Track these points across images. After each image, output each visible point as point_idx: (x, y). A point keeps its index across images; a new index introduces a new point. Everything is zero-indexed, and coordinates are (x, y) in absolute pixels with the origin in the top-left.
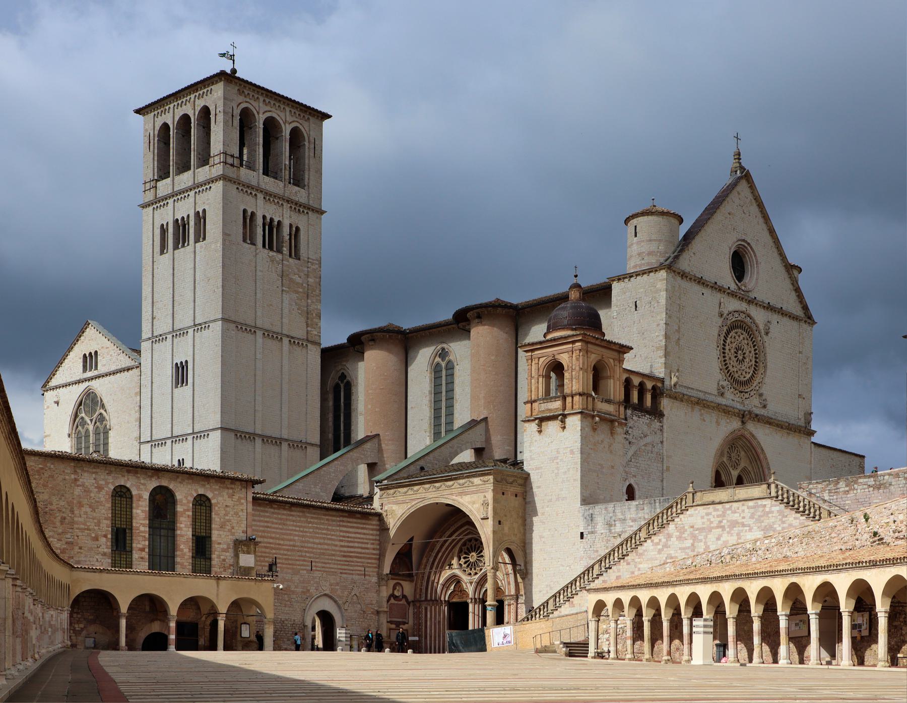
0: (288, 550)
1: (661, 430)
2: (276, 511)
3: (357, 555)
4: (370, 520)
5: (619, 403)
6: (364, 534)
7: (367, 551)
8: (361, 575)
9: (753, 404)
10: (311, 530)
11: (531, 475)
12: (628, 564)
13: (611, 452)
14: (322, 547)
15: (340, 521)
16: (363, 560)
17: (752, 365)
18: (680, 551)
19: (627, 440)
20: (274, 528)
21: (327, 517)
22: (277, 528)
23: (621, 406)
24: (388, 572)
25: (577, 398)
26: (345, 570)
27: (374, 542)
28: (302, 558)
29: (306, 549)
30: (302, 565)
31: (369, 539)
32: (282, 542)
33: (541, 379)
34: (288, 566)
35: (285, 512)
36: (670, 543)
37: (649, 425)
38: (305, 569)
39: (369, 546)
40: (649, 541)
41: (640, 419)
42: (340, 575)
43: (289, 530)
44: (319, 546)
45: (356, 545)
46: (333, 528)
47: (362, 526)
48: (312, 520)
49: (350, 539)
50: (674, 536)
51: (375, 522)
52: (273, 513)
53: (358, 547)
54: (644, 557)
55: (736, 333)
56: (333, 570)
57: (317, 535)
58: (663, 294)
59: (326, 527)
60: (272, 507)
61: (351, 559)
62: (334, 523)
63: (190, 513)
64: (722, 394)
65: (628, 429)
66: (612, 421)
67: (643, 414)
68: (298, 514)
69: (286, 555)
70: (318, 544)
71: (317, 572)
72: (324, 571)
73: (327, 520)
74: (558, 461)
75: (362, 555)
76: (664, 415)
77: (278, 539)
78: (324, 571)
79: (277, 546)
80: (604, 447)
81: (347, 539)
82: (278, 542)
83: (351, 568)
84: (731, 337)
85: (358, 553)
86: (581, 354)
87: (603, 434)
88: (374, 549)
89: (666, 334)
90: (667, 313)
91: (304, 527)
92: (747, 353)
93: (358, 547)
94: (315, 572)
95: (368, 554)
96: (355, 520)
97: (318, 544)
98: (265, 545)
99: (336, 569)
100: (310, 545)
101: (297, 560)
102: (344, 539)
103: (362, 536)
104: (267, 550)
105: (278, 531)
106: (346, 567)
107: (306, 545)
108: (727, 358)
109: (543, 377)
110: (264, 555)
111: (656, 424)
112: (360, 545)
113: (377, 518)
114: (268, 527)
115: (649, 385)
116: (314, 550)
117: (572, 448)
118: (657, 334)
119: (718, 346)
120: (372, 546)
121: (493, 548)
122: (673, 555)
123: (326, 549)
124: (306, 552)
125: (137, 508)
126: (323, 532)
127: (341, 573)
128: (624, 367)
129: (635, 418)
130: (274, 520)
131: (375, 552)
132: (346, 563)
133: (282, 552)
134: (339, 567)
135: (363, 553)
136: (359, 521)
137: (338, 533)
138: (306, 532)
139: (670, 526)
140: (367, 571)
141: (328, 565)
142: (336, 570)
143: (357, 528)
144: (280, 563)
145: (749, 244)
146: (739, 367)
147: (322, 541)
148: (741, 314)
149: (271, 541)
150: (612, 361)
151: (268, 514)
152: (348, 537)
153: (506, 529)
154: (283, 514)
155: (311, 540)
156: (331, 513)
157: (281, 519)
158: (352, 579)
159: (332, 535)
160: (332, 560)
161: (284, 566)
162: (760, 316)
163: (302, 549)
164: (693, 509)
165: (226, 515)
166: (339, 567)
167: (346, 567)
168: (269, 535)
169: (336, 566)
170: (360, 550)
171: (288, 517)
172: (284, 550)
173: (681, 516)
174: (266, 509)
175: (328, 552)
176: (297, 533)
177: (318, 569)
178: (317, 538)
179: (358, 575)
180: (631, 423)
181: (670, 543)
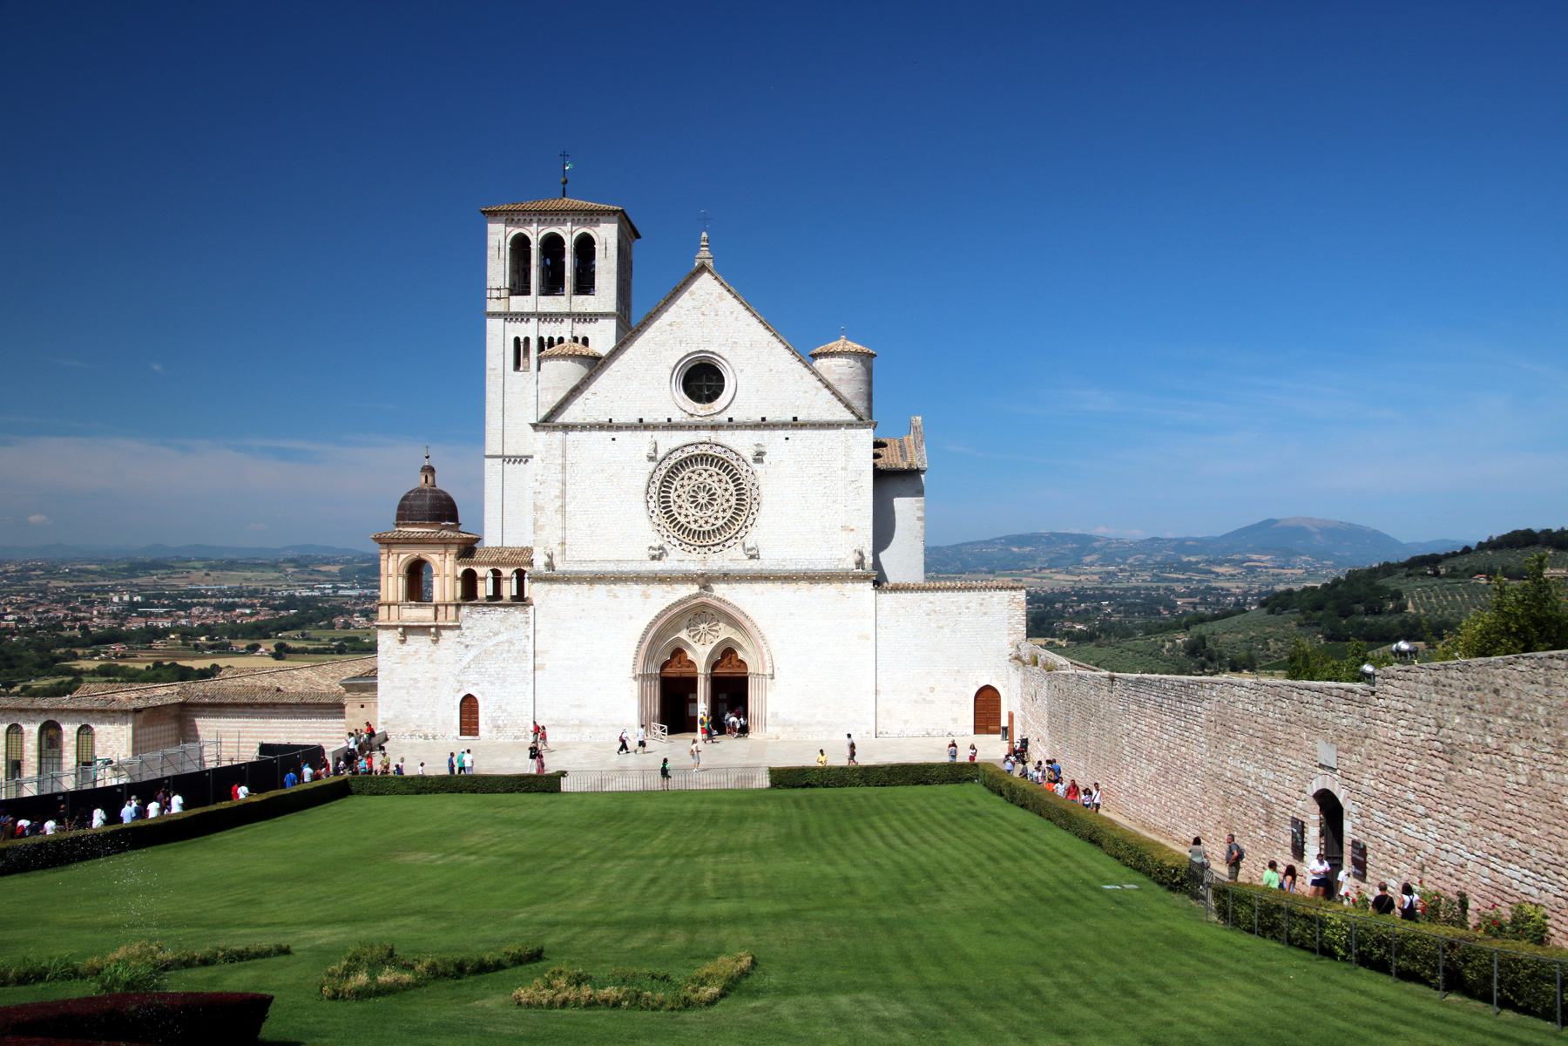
1: (527, 623)
9: (729, 558)
13: (432, 662)
17: (730, 507)
19: (462, 643)
33: (400, 579)
37: (502, 621)
41: (487, 616)
55: (693, 472)
63: (75, 743)
64: (653, 558)
84: (683, 479)
87: (418, 643)
92: (719, 492)
108: (674, 508)
111: (516, 615)
119: (651, 497)
125: (28, 742)
129: (476, 616)
145: (713, 353)
146: (701, 514)
147: (314, 735)
148: (700, 447)
149: (251, 740)
162: (742, 443)
165: (107, 741)
178: (308, 732)
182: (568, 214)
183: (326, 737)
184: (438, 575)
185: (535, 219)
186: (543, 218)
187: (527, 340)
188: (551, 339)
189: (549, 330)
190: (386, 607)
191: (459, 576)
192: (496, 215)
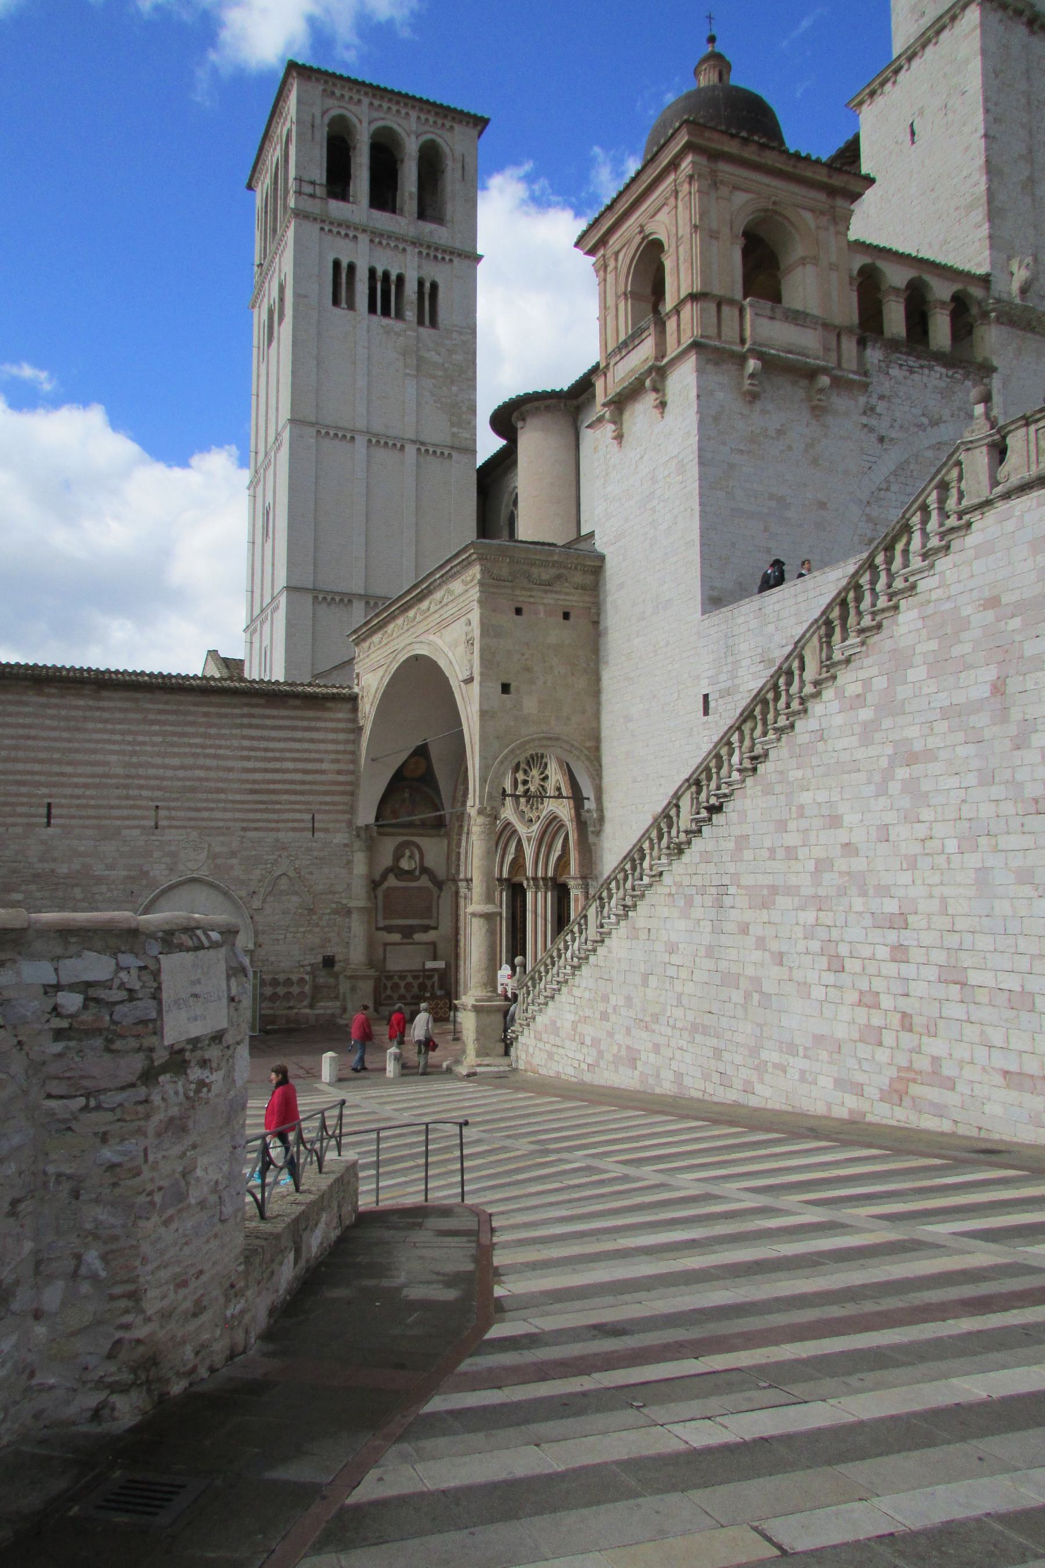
0: (86, 786)
2: (53, 701)
3: (294, 787)
4: (330, 709)
5: (839, 332)
6: (312, 741)
7: (318, 777)
8: (303, 830)
10: (160, 739)
11: (607, 559)
12: (768, 791)
13: (815, 462)
14: (189, 773)
15: (243, 716)
16: (310, 798)
18: (942, 726)
19: (872, 430)
20: (44, 739)
21: (205, 709)
22: (56, 740)
23: (844, 339)
24: (371, 819)
25: (687, 311)
26: (258, 821)
27: (339, 757)
28: (131, 802)
29: (142, 782)
30: (128, 818)
31: (327, 752)
32: (69, 769)
34: (87, 822)
35: (81, 703)
36: (902, 692)
38: (138, 827)
39: (325, 766)
40: (828, 694)
42: (242, 833)
43: (89, 741)
44: (181, 773)
45: (289, 765)
46: (223, 731)
47: (305, 724)
48: (159, 717)
49: (270, 755)
50: (918, 659)
51: (342, 713)
52: (46, 706)
53: (296, 771)
54: (815, 760)
56: (221, 824)
57: (176, 750)
58: (976, 65)
59: (202, 730)
60: (40, 694)
61: (274, 797)
62: (224, 721)
65: (874, 401)
66: (811, 374)
67: (924, 363)
68: (119, 704)
69: (78, 797)
70: (175, 768)
71: (173, 831)
72: (192, 827)
73: (206, 715)
74: (656, 501)
75: (307, 787)
76: (994, 370)
77: (52, 761)
78: (192, 827)
79: (56, 779)
80: (790, 448)
81: (263, 754)
82: (56, 769)
83: (275, 816)
85: (292, 782)
86: (695, 186)
88: (339, 772)
89: (987, 161)
90: (987, 111)
91: (136, 733)
93: (296, 771)
94: (167, 831)
95: (322, 783)
96: (286, 713)
97: (175, 768)
98: (19, 777)
99: (229, 820)
100: (152, 772)
101: (112, 807)
102: (252, 754)
103: (305, 746)
104: (24, 790)
105: (58, 744)
106: (258, 816)
107: (141, 771)
109: (626, 299)
110: (14, 800)
112: (300, 765)
113: (349, 706)
114: (29, 738)
115: (942, 291)
116: (165, 783)
117: (680, 457)
118: (965, 173)
120: (335, 767)
121: (482, 758)
122: (918, 746)
123: (200, 779)
124: (141, 787)
126: (192, 741)
127: (244, 829)
128: (853, 235)
129: (895, 371)
130: (48, 722)
131: (341, 778)
132: (262, 806)
133: (68, 791)
134: (238, 815)
135: (310, 783)
136: (298, 713)
137: (235, 743)
138: (144, 743)
139: (901, 618)
140: (320, 821)
141: (206, 814)
142: (230, 824)
143: (294, 728)
144: (61, 816)
147: (190, 761)
149: (37, 767)
150: (808, 216)
151: (30, 709)
152: (266, 750)
153: (530, 705)
154: (77, 708)
155: (159, 761)
156: (216, 699)
157: (67, 719)
158: (277, 840)
159: (220, 747)
160: (219, 801)
161: (73, 822)
163: (129, 781)
164: (991, 515)
166: (238, 815)
167: (258, 816)
168: (32, 755)
169: (229, 815)
170: (298, 777)
171: (88, 714)
172: (76, 785)
173: (943, 563)
174: (25, 698)
175: (205, 784)
176: (116, 747)
177: (175, 823)
178: (175, 755)
179: (294, 830)
180: (881, 384)
181: (902, 692)
182: (413, 107)
183: (218, 768)
184: (815, 260)
185: (366, 101)
186: (376, 103)
187: (352, 268)
188: (386, 275)
189: (388, 262)
190: (713, 307)
191: (855, 273)
192: (309, 78)
